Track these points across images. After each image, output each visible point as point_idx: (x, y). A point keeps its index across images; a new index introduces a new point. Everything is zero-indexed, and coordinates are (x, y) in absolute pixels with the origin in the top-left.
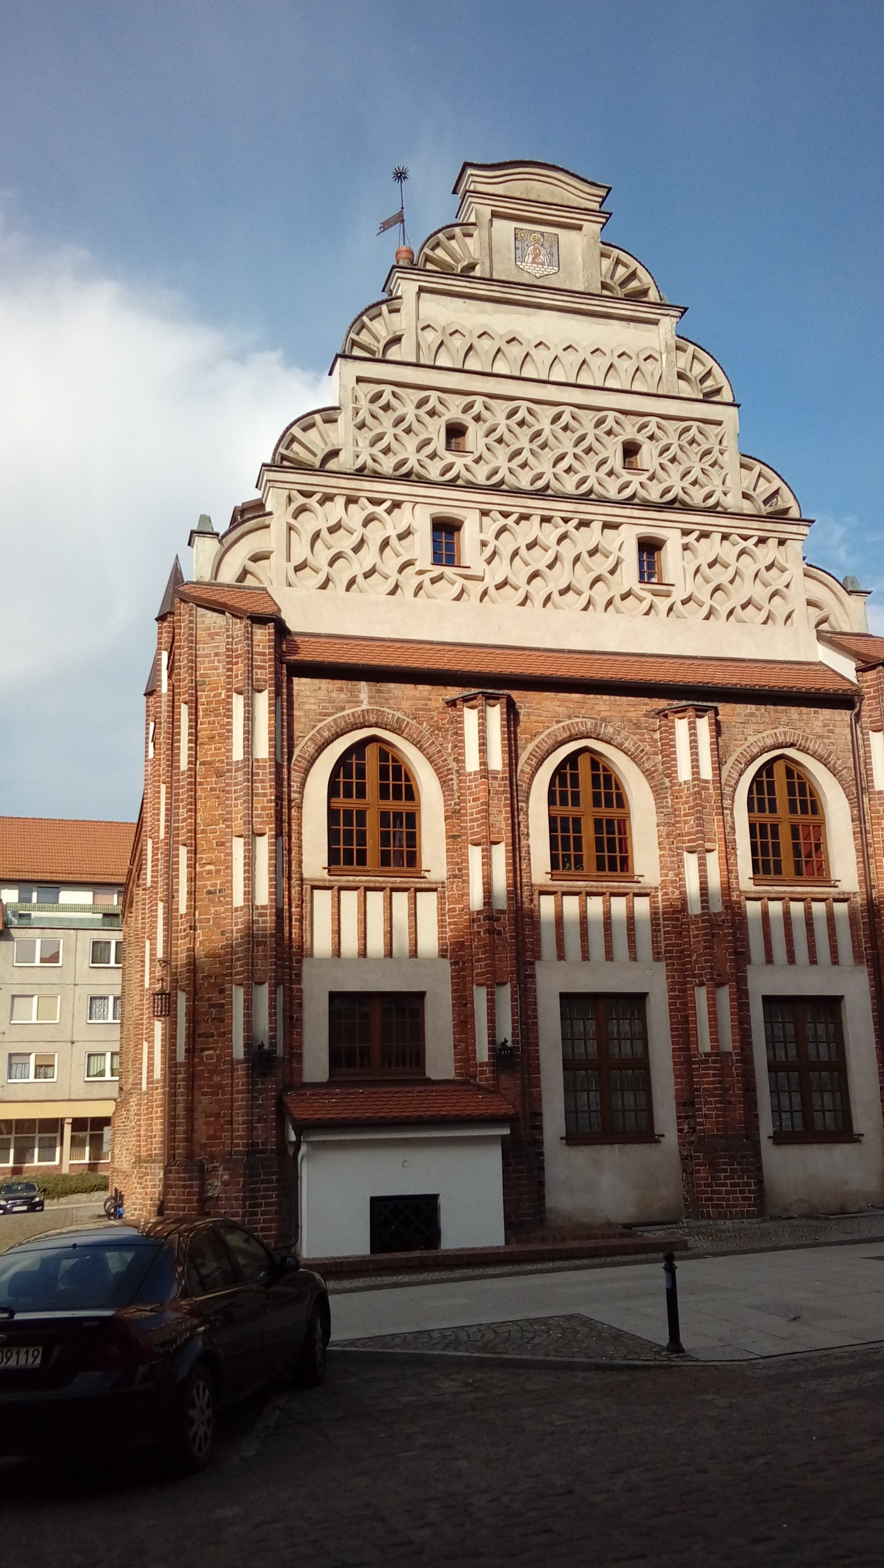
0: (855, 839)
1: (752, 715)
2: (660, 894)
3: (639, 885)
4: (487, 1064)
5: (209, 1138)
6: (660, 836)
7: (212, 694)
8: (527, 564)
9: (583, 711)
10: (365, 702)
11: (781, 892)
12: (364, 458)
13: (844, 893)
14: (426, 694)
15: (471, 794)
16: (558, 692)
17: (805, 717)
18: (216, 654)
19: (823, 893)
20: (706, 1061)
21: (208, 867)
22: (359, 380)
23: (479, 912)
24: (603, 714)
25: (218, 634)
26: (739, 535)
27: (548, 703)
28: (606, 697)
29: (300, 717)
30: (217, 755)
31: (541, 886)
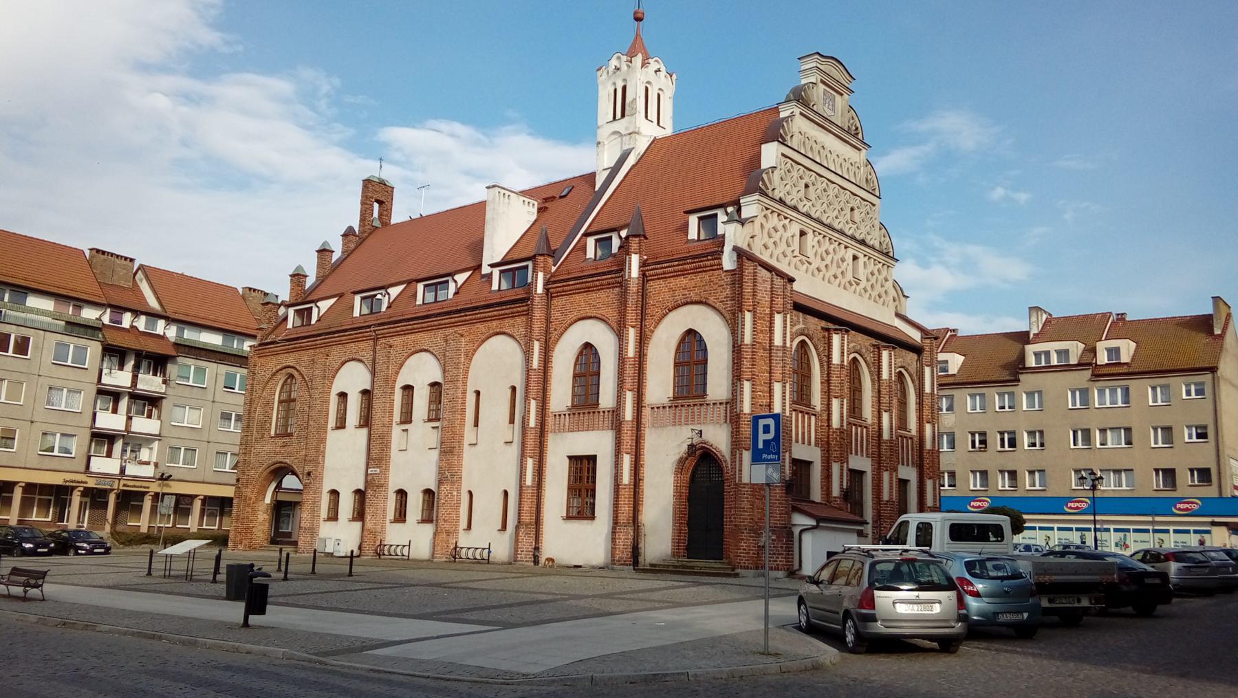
0: (916, 412)
2: (871, 428)
4: (838, 498)
5: (759, 519)
6: (873, 402)
7: (762, 309)
12: (782, 195)
14: (816, 323)
15: (835, 374)
18: (765, 291)
20: (887, 504)
21: (759, 393)
22: (783, 155)
23: (836, 429)
25: (766, 281)
28: (861, 334)
30: (764, 340)
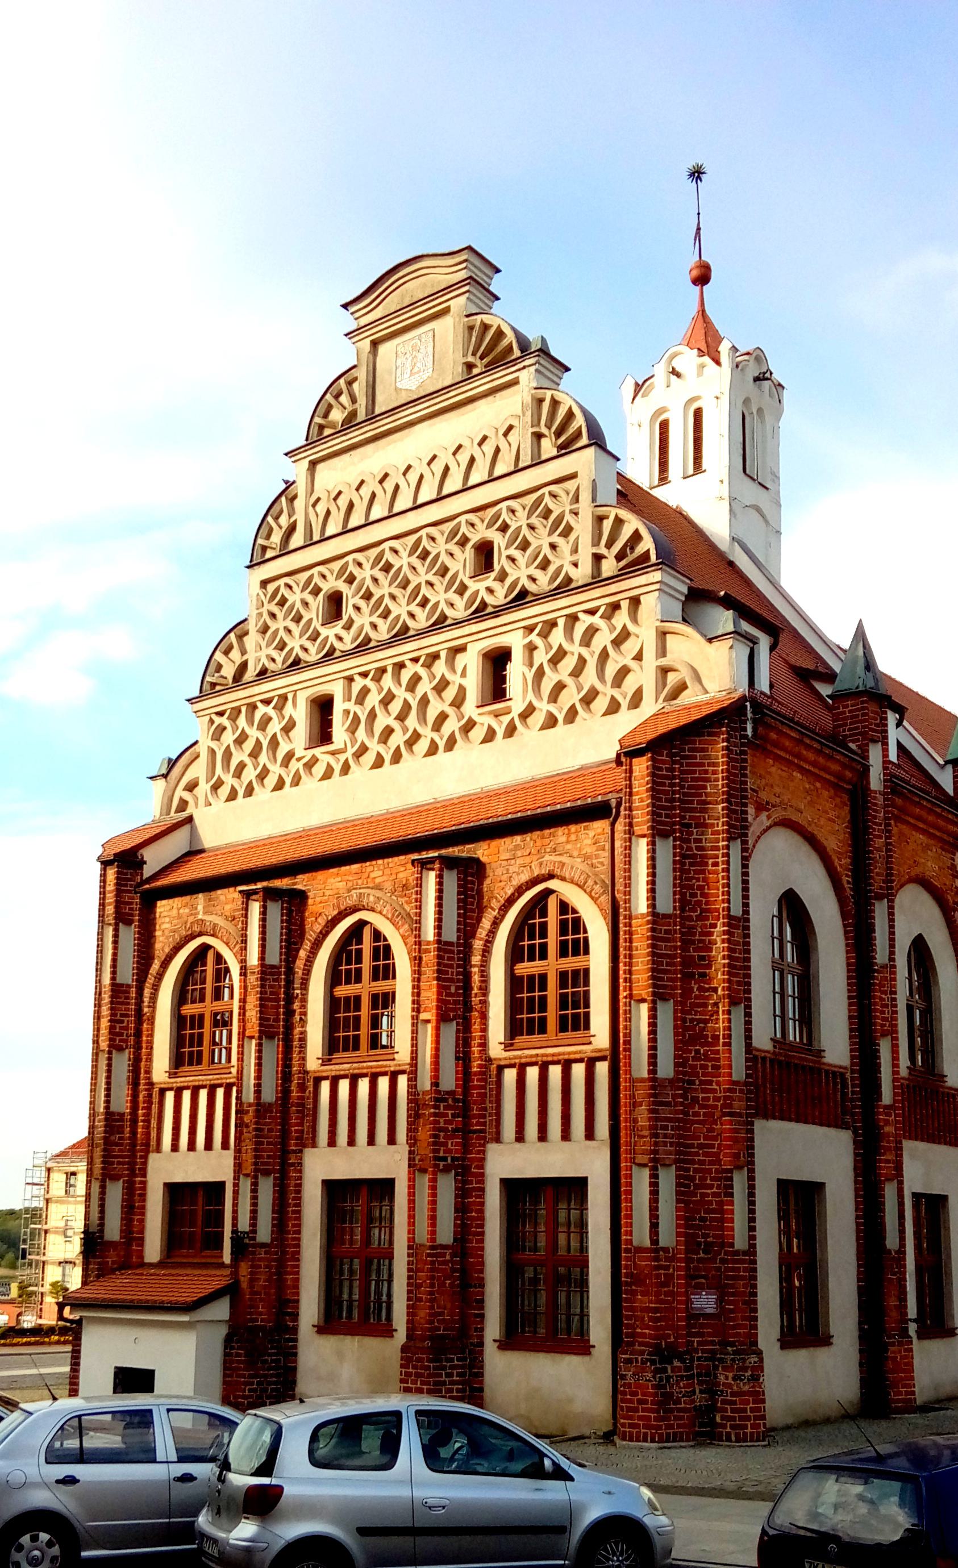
1: (517, 847)
3: (395, 1062)
8: (617, 662)
9: (360, 882)
10: (201, 913)
11: (531, 1056)
13: (600, 1050)
16: (340, 866)
17: (573, 837)
19: (575, 1053)
24: (377, 881)
26: (586, 612)
27: (332, 880)
28: (380, 862)
29: (159, 936)
31: (315, 1072)
